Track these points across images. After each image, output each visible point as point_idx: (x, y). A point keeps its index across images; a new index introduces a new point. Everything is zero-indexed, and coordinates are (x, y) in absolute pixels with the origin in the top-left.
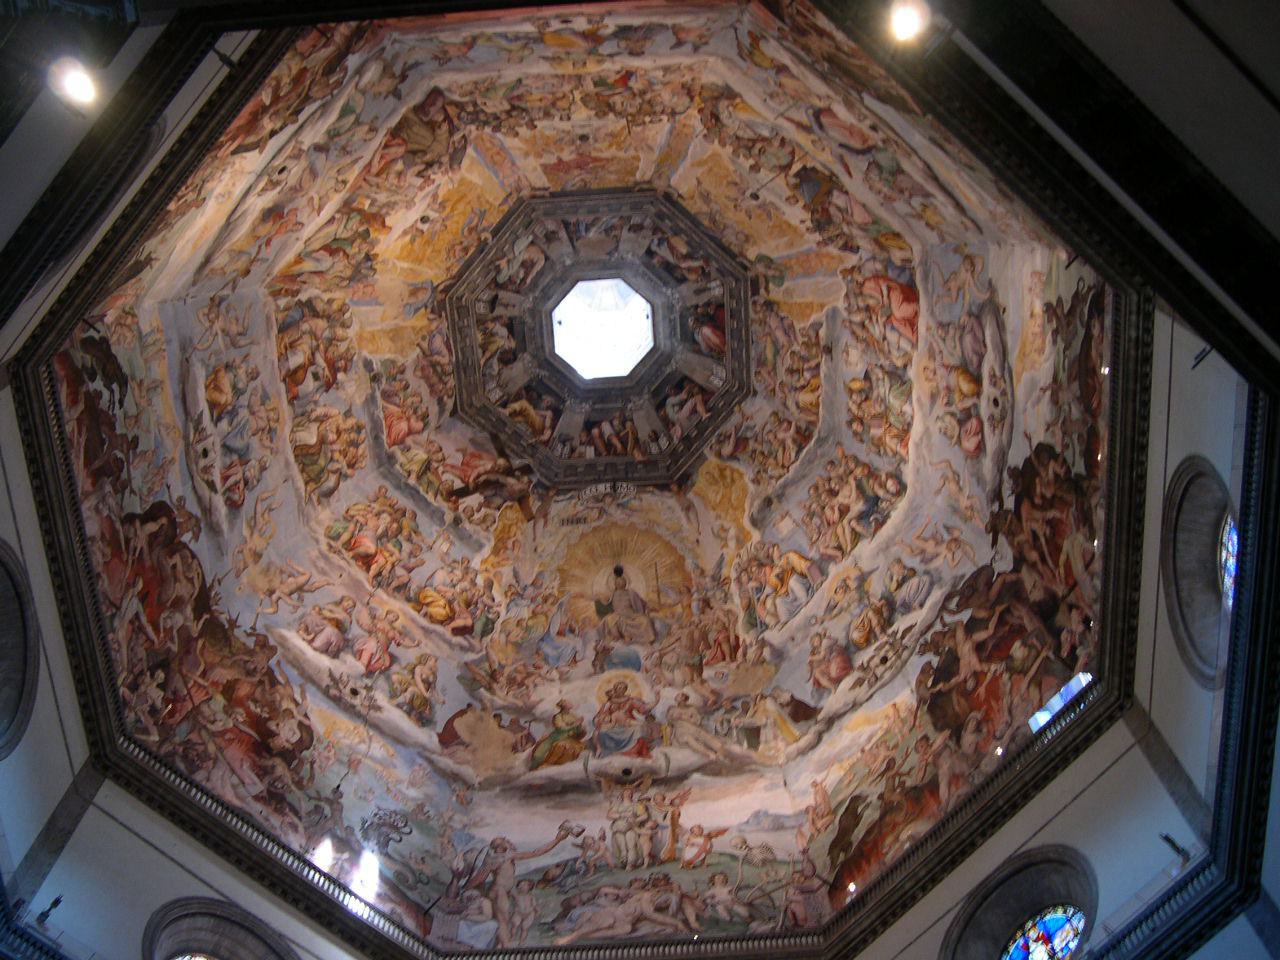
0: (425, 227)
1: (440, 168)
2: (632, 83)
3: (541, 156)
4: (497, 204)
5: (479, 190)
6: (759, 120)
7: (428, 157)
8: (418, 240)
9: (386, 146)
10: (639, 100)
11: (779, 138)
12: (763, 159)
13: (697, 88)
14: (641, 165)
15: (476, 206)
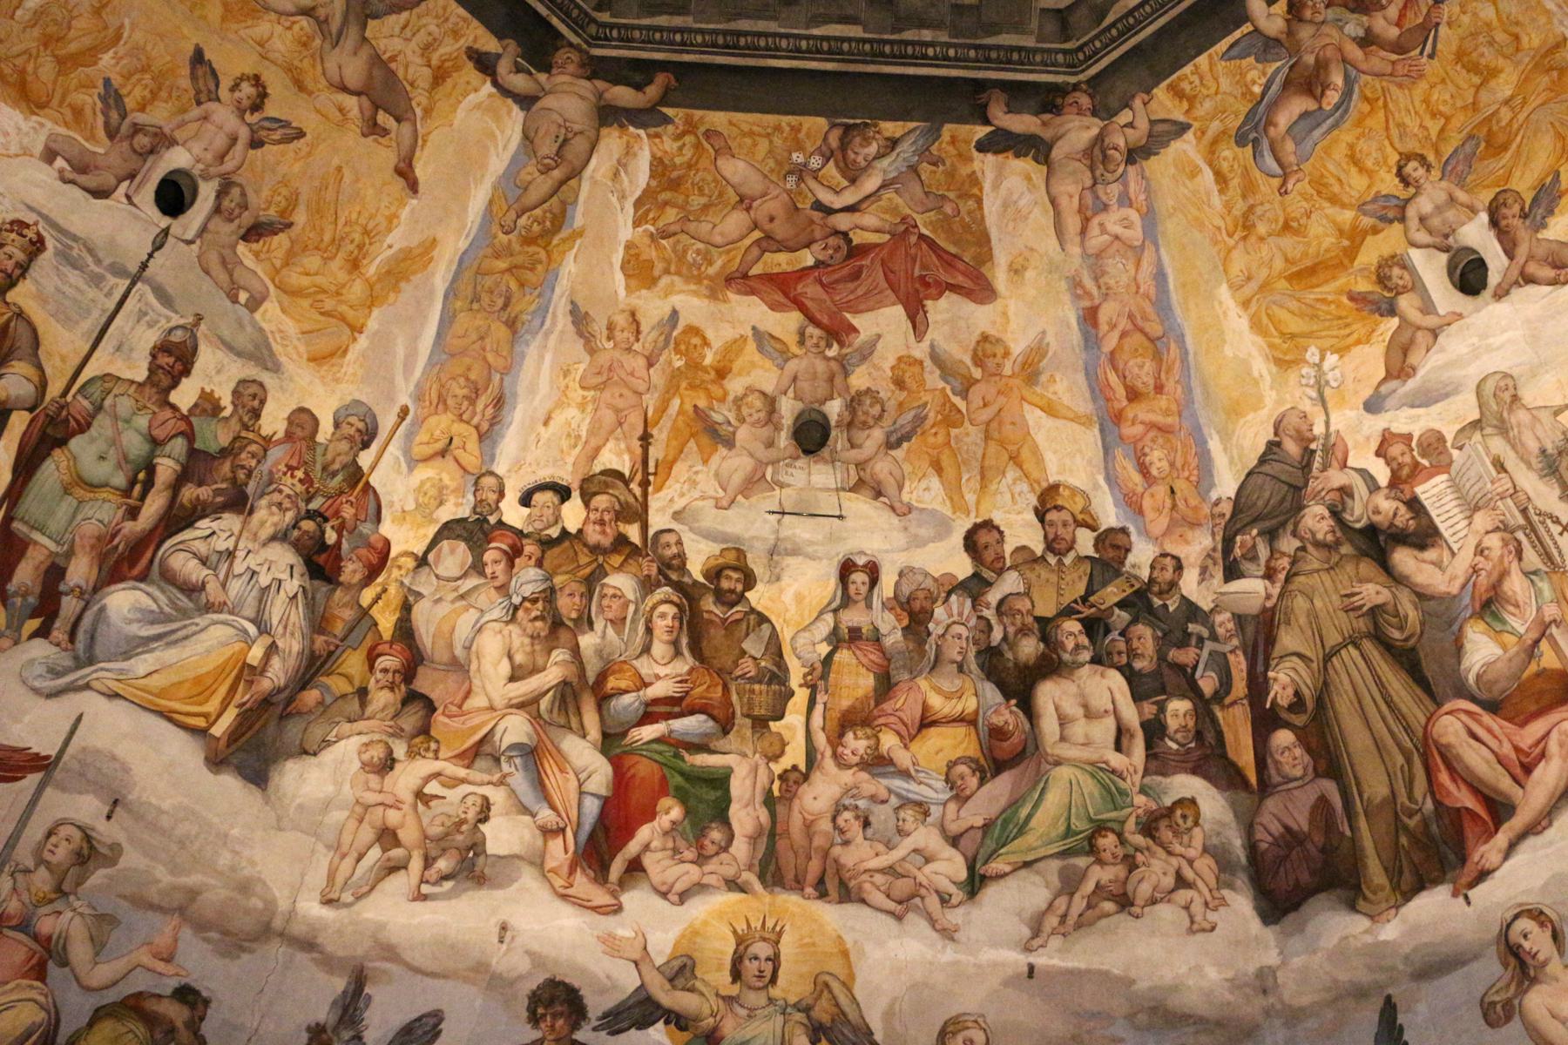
0: (1476, 234)
1: (1345, 492)
2: (600, 775)
3: (986, 349)
4: (1186, 147)
5: (1239, 262)
6: (141, 665)
7: (1373, 592)
8: (1524, 184)
9: (1498, 809)
10: (587, 641)
11: (69, 606)
12: (135, 445)
13: (382, 699)
14: (625, 231)
15: (1267, 187)
